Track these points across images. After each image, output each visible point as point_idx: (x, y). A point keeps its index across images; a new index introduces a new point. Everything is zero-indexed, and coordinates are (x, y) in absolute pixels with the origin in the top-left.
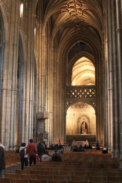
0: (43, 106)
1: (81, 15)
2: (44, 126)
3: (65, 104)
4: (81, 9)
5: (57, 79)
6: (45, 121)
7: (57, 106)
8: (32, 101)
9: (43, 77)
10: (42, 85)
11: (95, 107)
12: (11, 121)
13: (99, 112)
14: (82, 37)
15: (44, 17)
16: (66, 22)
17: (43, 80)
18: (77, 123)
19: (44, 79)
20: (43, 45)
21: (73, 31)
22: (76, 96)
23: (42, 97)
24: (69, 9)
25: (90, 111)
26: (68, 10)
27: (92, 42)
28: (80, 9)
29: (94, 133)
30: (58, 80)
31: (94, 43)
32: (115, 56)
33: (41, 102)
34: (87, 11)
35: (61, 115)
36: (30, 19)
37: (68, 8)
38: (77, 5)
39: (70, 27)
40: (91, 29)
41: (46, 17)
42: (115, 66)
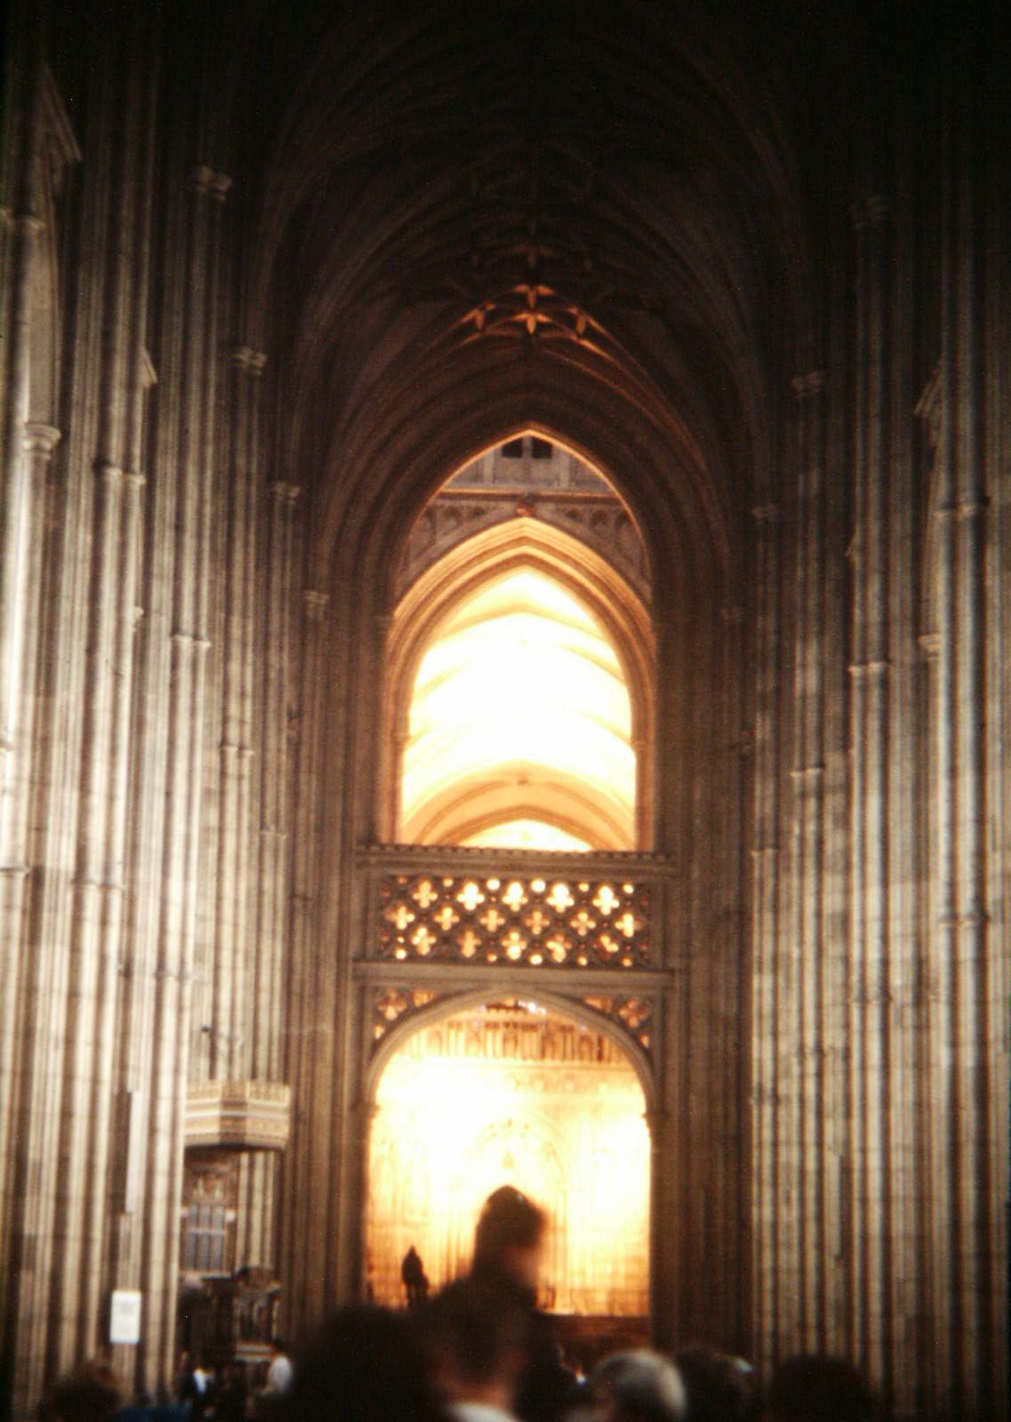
0: (224, 1029)
3: (369, 1016)
5: (303, 777)
6: (238, 1168)
7: (294, 1030)
9: (232, 751)
11: (647, 1053)
13: (685, 1099)
17: (231, 785)
20: (241, 461)
22: (469, 945)
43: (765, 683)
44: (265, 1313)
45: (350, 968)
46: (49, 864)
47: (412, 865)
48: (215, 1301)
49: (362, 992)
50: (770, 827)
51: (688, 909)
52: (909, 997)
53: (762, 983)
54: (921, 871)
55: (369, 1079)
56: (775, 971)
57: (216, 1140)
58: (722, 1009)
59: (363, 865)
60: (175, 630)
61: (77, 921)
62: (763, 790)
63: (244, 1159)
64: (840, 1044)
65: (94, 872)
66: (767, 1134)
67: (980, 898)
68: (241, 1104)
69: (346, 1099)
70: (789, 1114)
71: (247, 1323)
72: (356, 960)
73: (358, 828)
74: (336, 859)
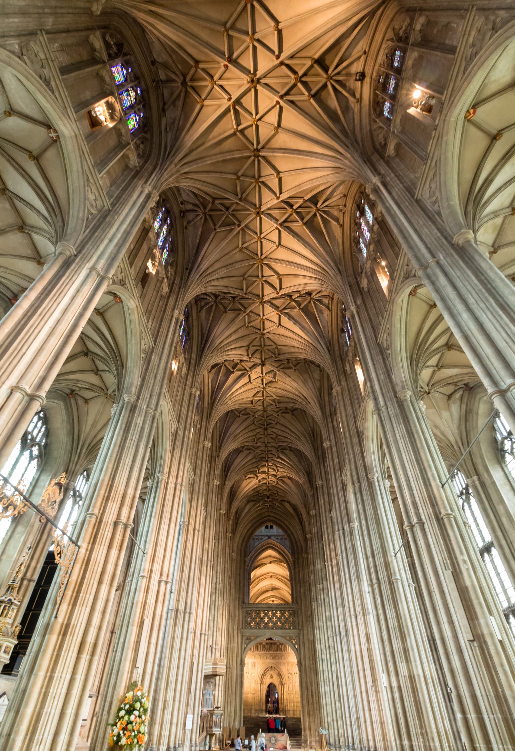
0: (214, 646)
1: (274, 484)
4: (276, 476)
8: (205, 635)
10: (215, 601)
14: (272, 517)
15: (224, 484)
16: (252, 493)
18: (258, 685)
21: (259, 506)
22: (262, 625)
23: (213, 627)
24: (258, 475)
26: (257, 476)
27: (287, 526)
28: (275, 476)
29: (292, 712)
30: (233, 591)
31: (291, 528)
32: (371, 560)
33: (211, 637)
34: (284, 479)
35: (235, 665)
36: (211, 487)
37: (259, 473)
38: (270, 470)
39: (255, 501)
40: (287, 505)
42: (374, 576)
43: (311, 568)
46: (179, 608)
49: (242, 636)
53: (317, 631)
54: (343, 606)
55: (243, 657)
57: (211, 673)
59: (242, 608)
62: (313, 589)
63: (218, 678)
67: (355, 610)
68: (216, 664)
69: (239, 662)
70: (325, 663)
71: (216, 722)
73: (241, 600)
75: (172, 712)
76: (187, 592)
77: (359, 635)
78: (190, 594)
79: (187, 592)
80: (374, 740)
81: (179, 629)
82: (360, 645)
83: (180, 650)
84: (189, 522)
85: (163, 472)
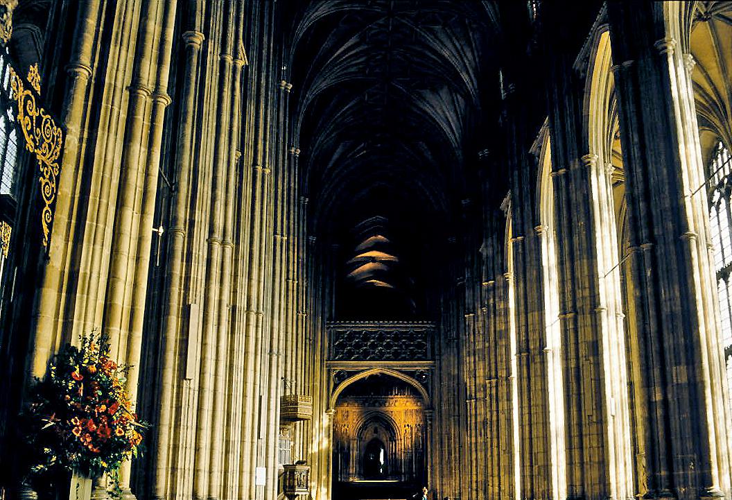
0: (289, 378)
2: (292, 443)
12: (244, 413)
19: (293, 291)
20: (292, 185)
25: (396, 404)
41: (304, 97)
44: (305, 478)
45: (325, 362)
47: (345, 327)
48: (288, 473)
49: (329, 371)
50: (471, 307)
51: (440, 339)
52: (537, 352)
56: (474, 355)
58: (452, 373)
59: (328, 328)
60: (275, 233)
61: (248, 325)
64: (504, 375)
65: (254, 307)
66: (473, 412)
68: (297, 404)
72: (326, 360)
73: (327, 315)
74: (320, 327)
75: (241, 456)
76: (250, 279)
77: (577, 344)
78: (254, 283)
79: (250, 279)
80: (583, 485)
81: (240, 337)
82: (577, 358)
83: (245, 370)
84: (243, 154)
85: (192, 28)
